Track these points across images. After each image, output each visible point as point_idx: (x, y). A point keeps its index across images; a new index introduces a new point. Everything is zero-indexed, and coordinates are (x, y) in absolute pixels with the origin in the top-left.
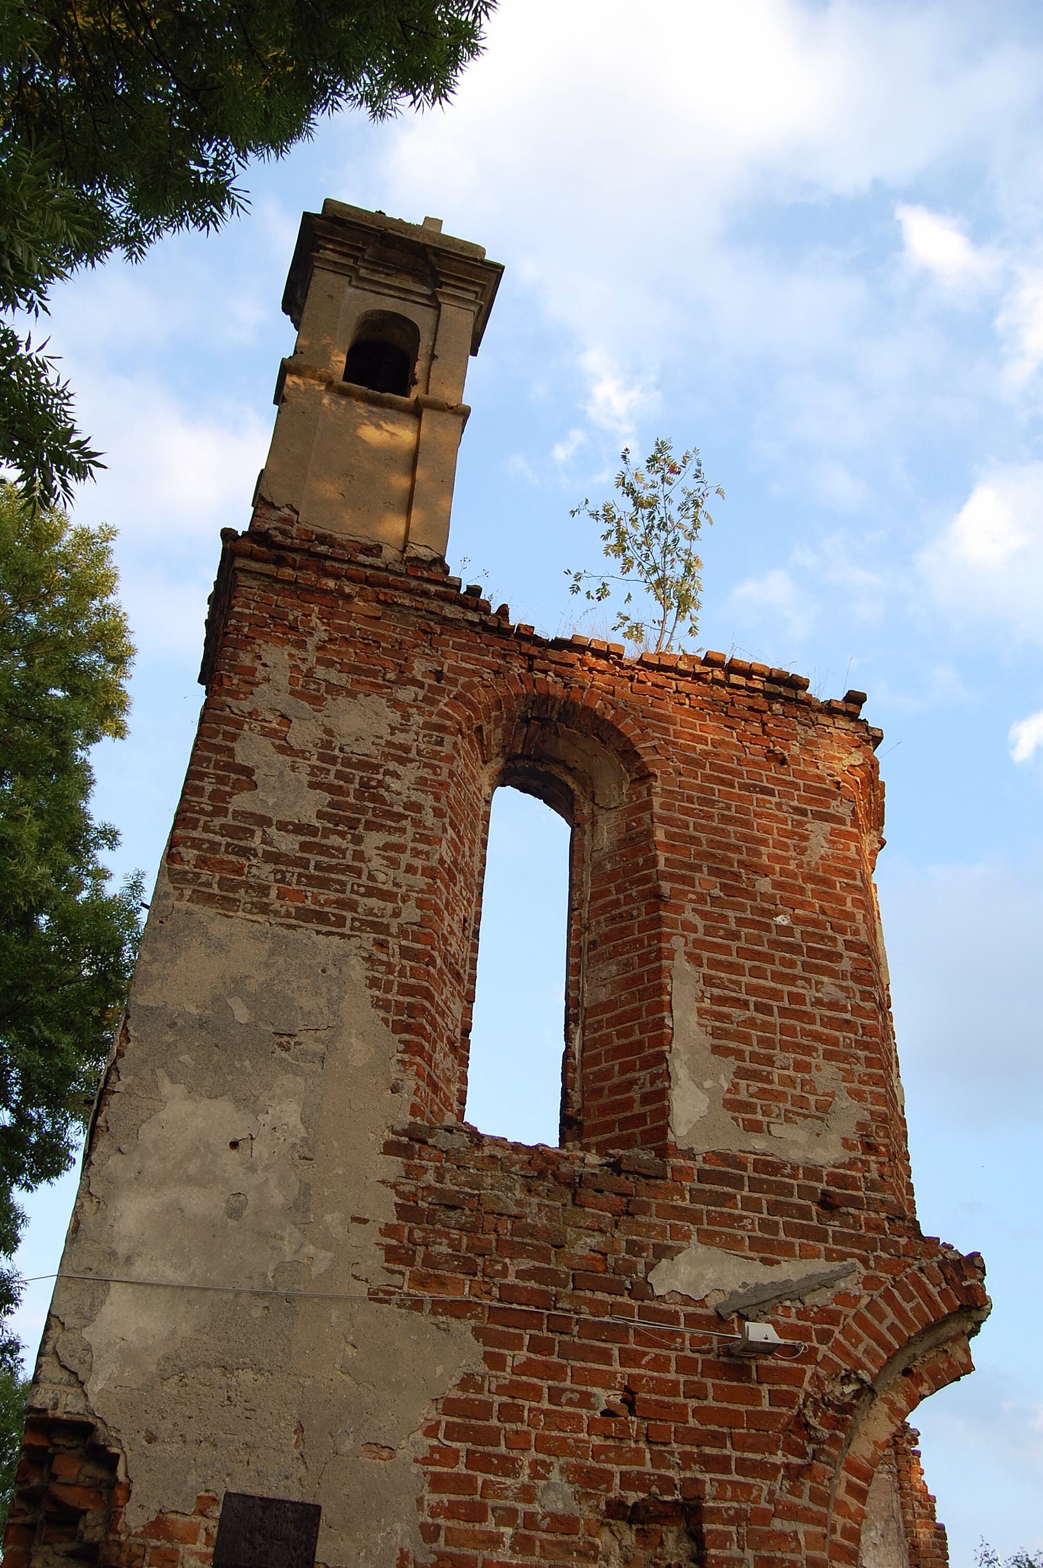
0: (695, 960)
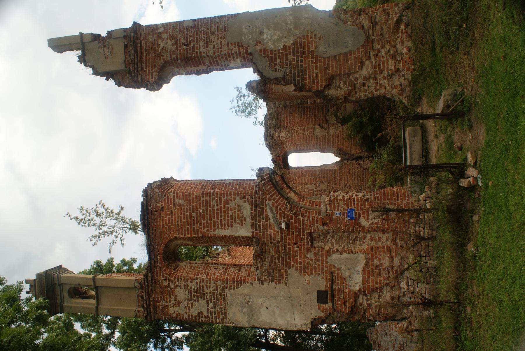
0: (214, 230)
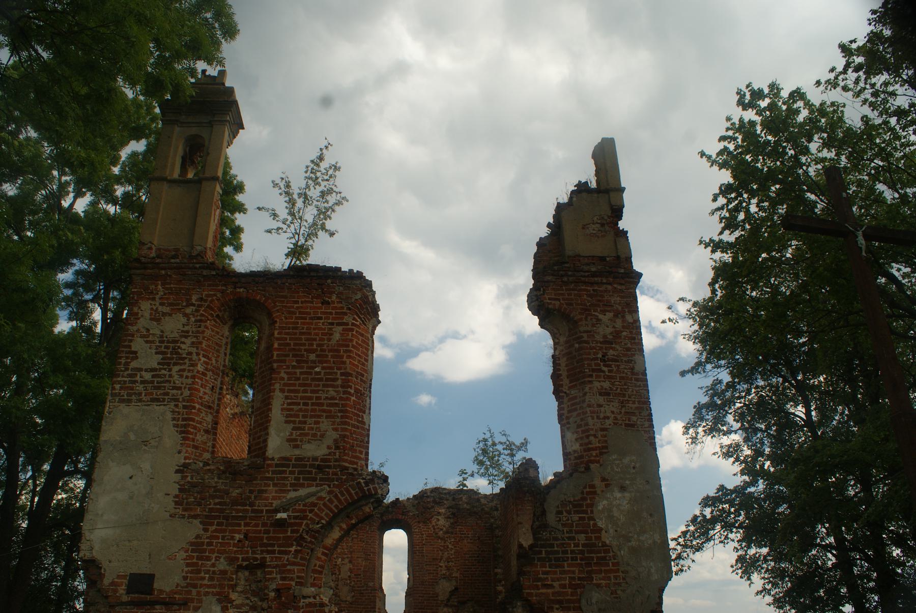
0: (282, 391)
